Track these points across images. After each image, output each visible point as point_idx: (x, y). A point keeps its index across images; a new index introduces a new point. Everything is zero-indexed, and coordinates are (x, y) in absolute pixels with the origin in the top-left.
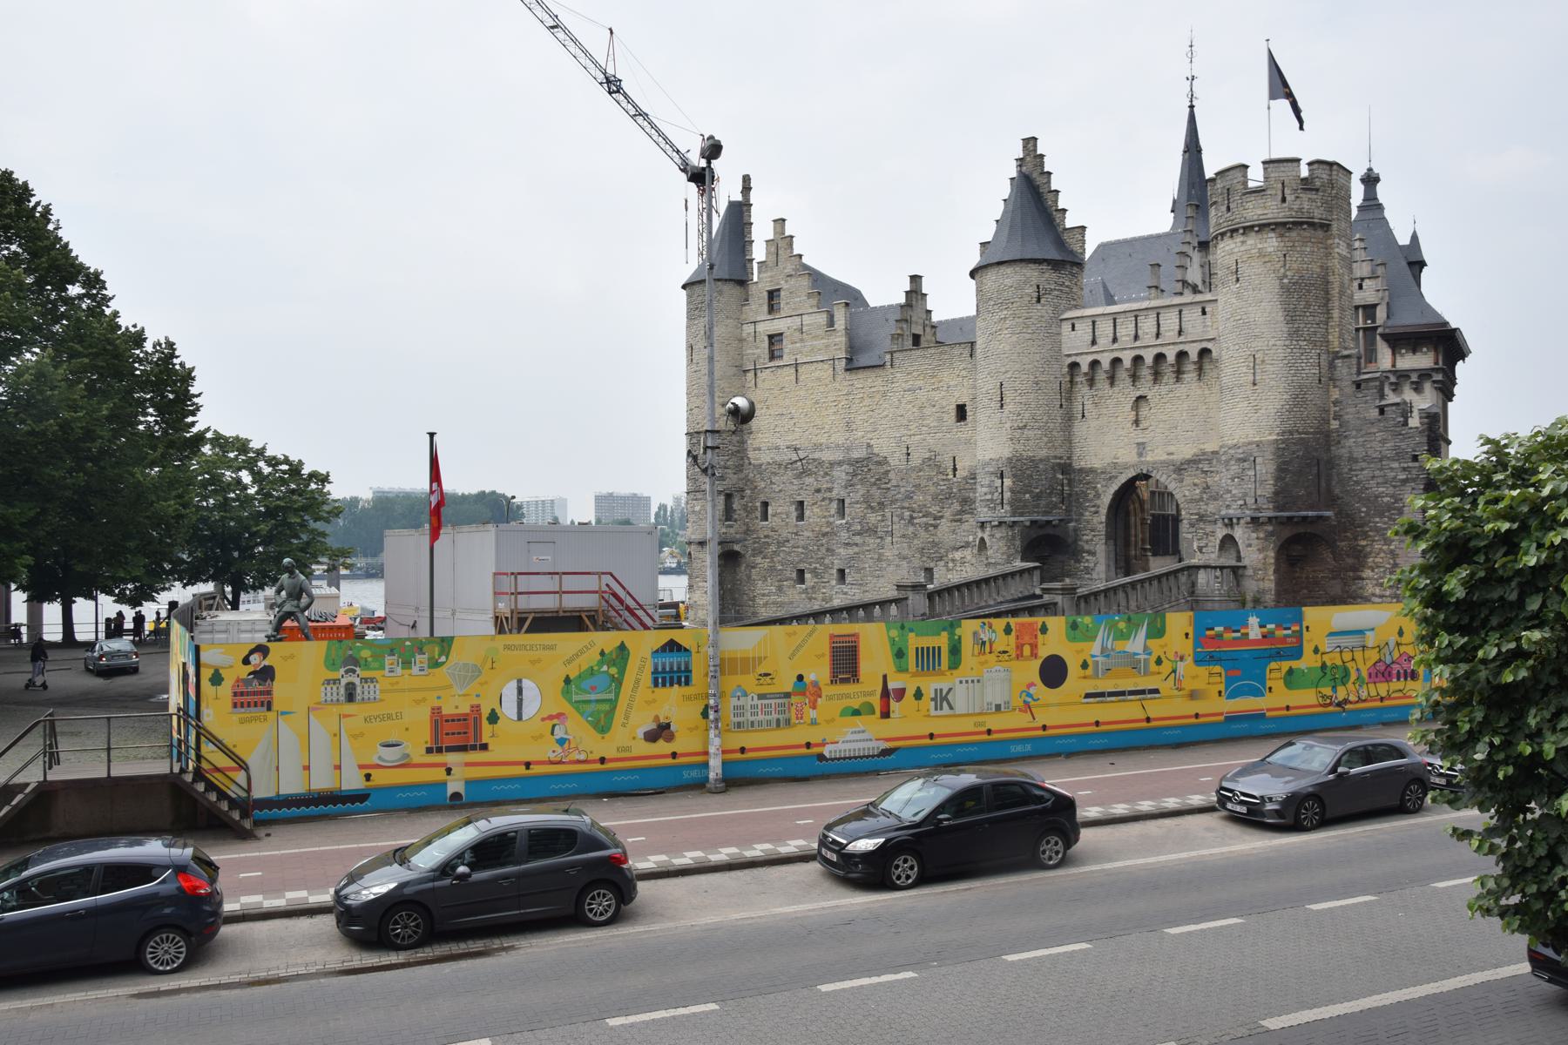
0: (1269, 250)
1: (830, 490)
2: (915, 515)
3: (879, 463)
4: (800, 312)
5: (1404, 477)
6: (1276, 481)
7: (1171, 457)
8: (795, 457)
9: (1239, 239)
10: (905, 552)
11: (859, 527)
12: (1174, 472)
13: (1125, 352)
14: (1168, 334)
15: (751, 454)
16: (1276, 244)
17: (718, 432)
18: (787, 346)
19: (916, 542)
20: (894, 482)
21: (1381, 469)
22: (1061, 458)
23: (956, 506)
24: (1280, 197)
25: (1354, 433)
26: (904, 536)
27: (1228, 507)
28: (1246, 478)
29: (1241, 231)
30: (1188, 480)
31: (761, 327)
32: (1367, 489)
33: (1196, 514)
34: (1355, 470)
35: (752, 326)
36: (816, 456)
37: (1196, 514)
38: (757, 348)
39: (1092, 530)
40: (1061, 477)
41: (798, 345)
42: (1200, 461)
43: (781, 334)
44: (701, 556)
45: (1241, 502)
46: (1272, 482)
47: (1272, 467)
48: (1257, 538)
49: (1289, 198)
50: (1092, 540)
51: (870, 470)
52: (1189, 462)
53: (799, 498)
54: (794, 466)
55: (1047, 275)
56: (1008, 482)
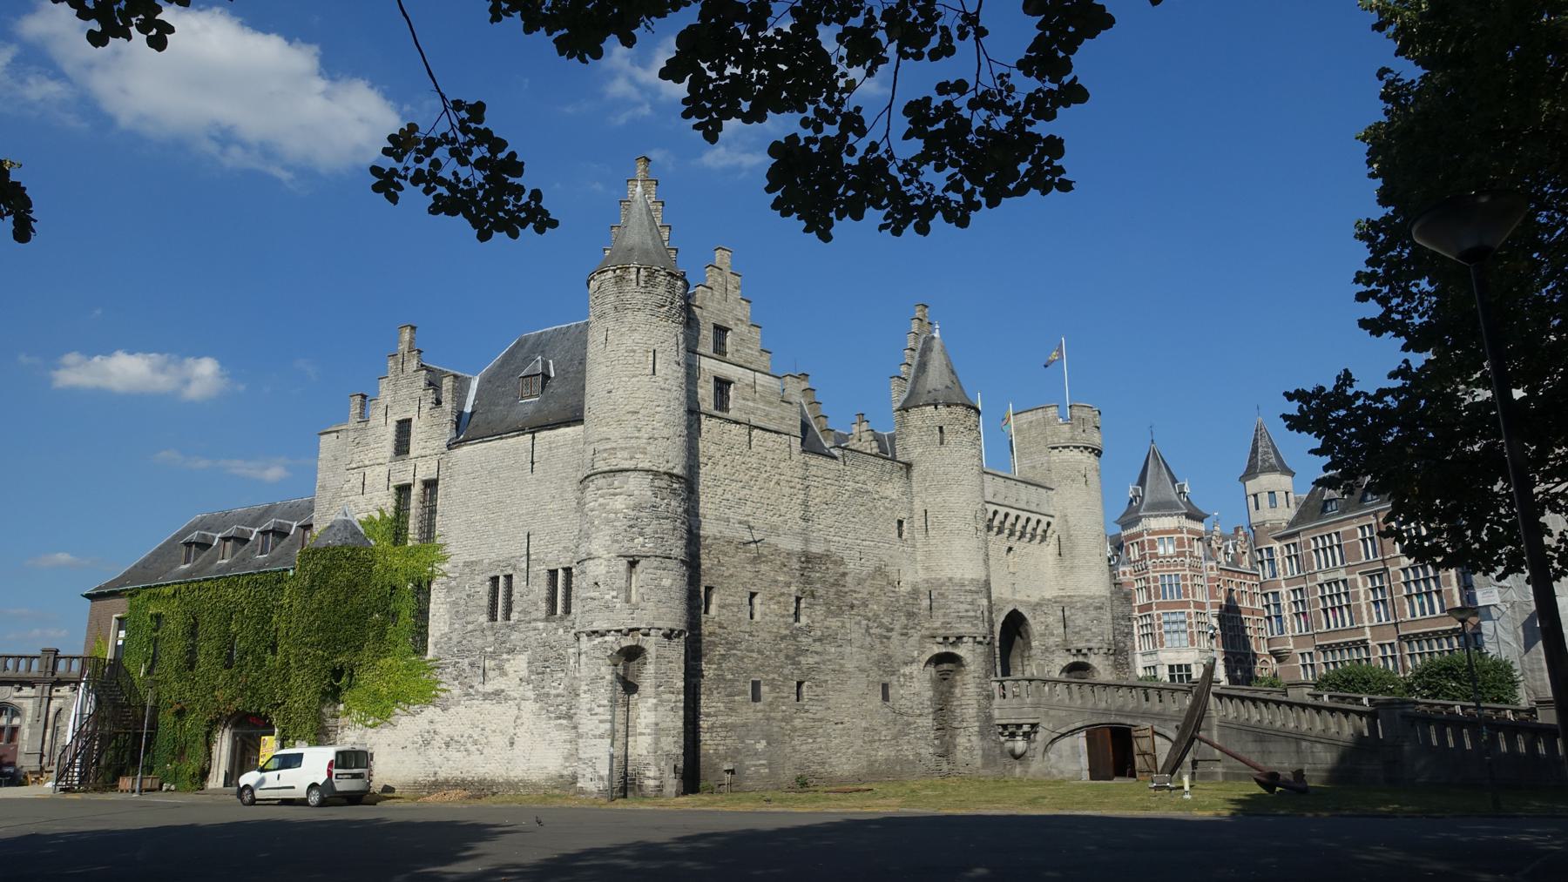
2: (871, 624)
3: (835, 562)
4: (753, 367)
8: (748, 538)
9: (1086, 453)
10: (865, 665)
11: (819, 633)
19: (873, 653)
23: (904, 620)
26: (862, 647)
27: (1088, 641)
36: (773, 540)
41: (751, 404)
42: (1041, 605)
43: (729, 383)
44: (667, 653)
45: (1100, 638)
51: (828, 568)
52: (1038, 604)
53: (754, 590)
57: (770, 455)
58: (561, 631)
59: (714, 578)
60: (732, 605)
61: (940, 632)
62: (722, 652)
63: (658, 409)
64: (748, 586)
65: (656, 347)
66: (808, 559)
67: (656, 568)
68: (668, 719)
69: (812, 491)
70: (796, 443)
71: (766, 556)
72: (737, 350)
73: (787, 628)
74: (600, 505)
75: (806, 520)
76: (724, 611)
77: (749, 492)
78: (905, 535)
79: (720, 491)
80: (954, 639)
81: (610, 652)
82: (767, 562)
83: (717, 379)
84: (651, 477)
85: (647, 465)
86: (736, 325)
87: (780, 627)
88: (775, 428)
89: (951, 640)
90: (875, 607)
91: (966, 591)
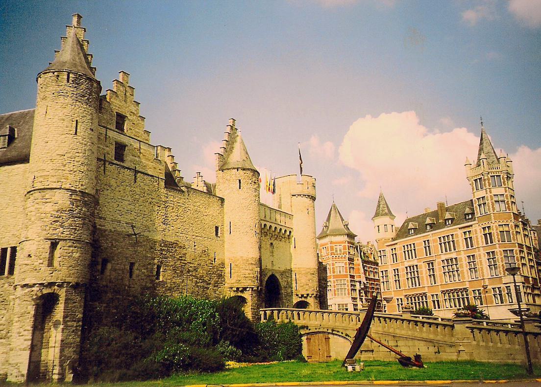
4: (139, 139)
8: (131, 231)
20: (188, 259)
36: (146, 234)
41: (136, 158)
43: (125, 146)
51: (176, 250)
52: (284, 272)
58: (6, 285)
60: (119, 270)
61: (234, 285)
62: (111, 297)
63: (77, 154)
65: (78, 119)
67: (69, 246)
68: (71, 337)
70: (163, 184)
71: (141, 243)
74: (36, 209)
77: (133, 207)
78: (219, 235)
79: (115, 206)
80: (242, 289)
81: (34, 297)
83: (117, 143)
84: (71, 193)
85: (68, 186)
87: (147, 282)
89: (240, 289)
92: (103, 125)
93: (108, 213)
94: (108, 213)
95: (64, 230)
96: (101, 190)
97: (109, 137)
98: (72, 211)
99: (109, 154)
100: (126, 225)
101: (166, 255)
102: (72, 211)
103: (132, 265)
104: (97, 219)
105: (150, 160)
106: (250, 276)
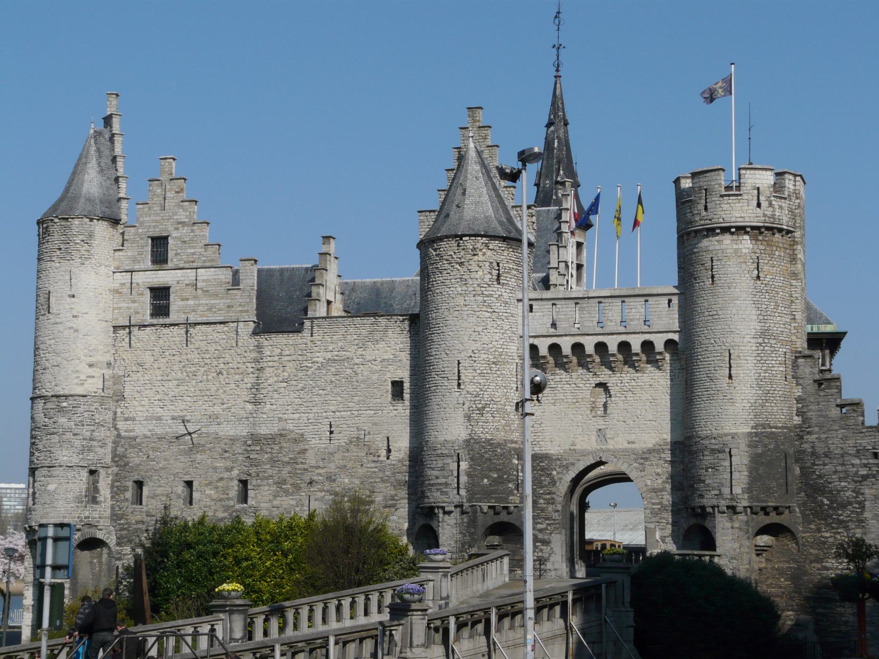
0: (744, 251)
1: (229, 469)
3: (295, 441)
4: (195, 265)
5: (865, 473)
6: (750, 473)
7: (633, 446)
12: (636, 460)
13: (587, 337)
14: (631, 323)
15: (121, 425)
16: (751, 246)
17: (86, 396)
18: (175, 303)
20: (313, 463)
21: (843, 465)
22: (516, 442)
24: (755, 203)
25: (817, 429)
28: (721, 469)
29: (718, 231)
30: (650, 470)
31: (139, 278)
32: (830, 483)
33: (658, 504)
34: (817, 465)
35: (130, 274)
36: (213, 429)
37: (658, 504)
38: (134, 302)
39: (546, 519)
40: (516, 462)
41: (191, 302)
45: (717, 492)
46: (746, 473)
47: (746, 461)
48: (732, 528)
49: (764, 204)
50: (546, 529)
52: (650, 451)
53: (188, 478)
54: (182, 440)
55: (505, 253)
56: (464, 465)
57: (211, 348)
59: (142, 473)
63: (53, 341)
64: (181, 475)
65: (51, 288)
66: (256, 439)
69: (268, 372)
71: (203, 446)
72: (176, 254)
73: (225, 511)
75: (256, 402)
76: (153, 501)
77: (186, 387)
82: (204, 451)
83: (152, 289)
84: (43, 401)
86: (177, 229)
88: (221, 319)
90: (346, 481)
91: (438, 456)
92: (127, 268)
93: (141, 409)
94: (141, 409)
95: (39, 455)
96: (126, 375)
97: (138, 284)
98: (45, 426)
99: (137, 313)
100: (172, 421)
101: (256, 459)
102: (45, 426)
103: (189, 484)
104: (121, 423)
105: (217, 295)
106: (439, 481)
